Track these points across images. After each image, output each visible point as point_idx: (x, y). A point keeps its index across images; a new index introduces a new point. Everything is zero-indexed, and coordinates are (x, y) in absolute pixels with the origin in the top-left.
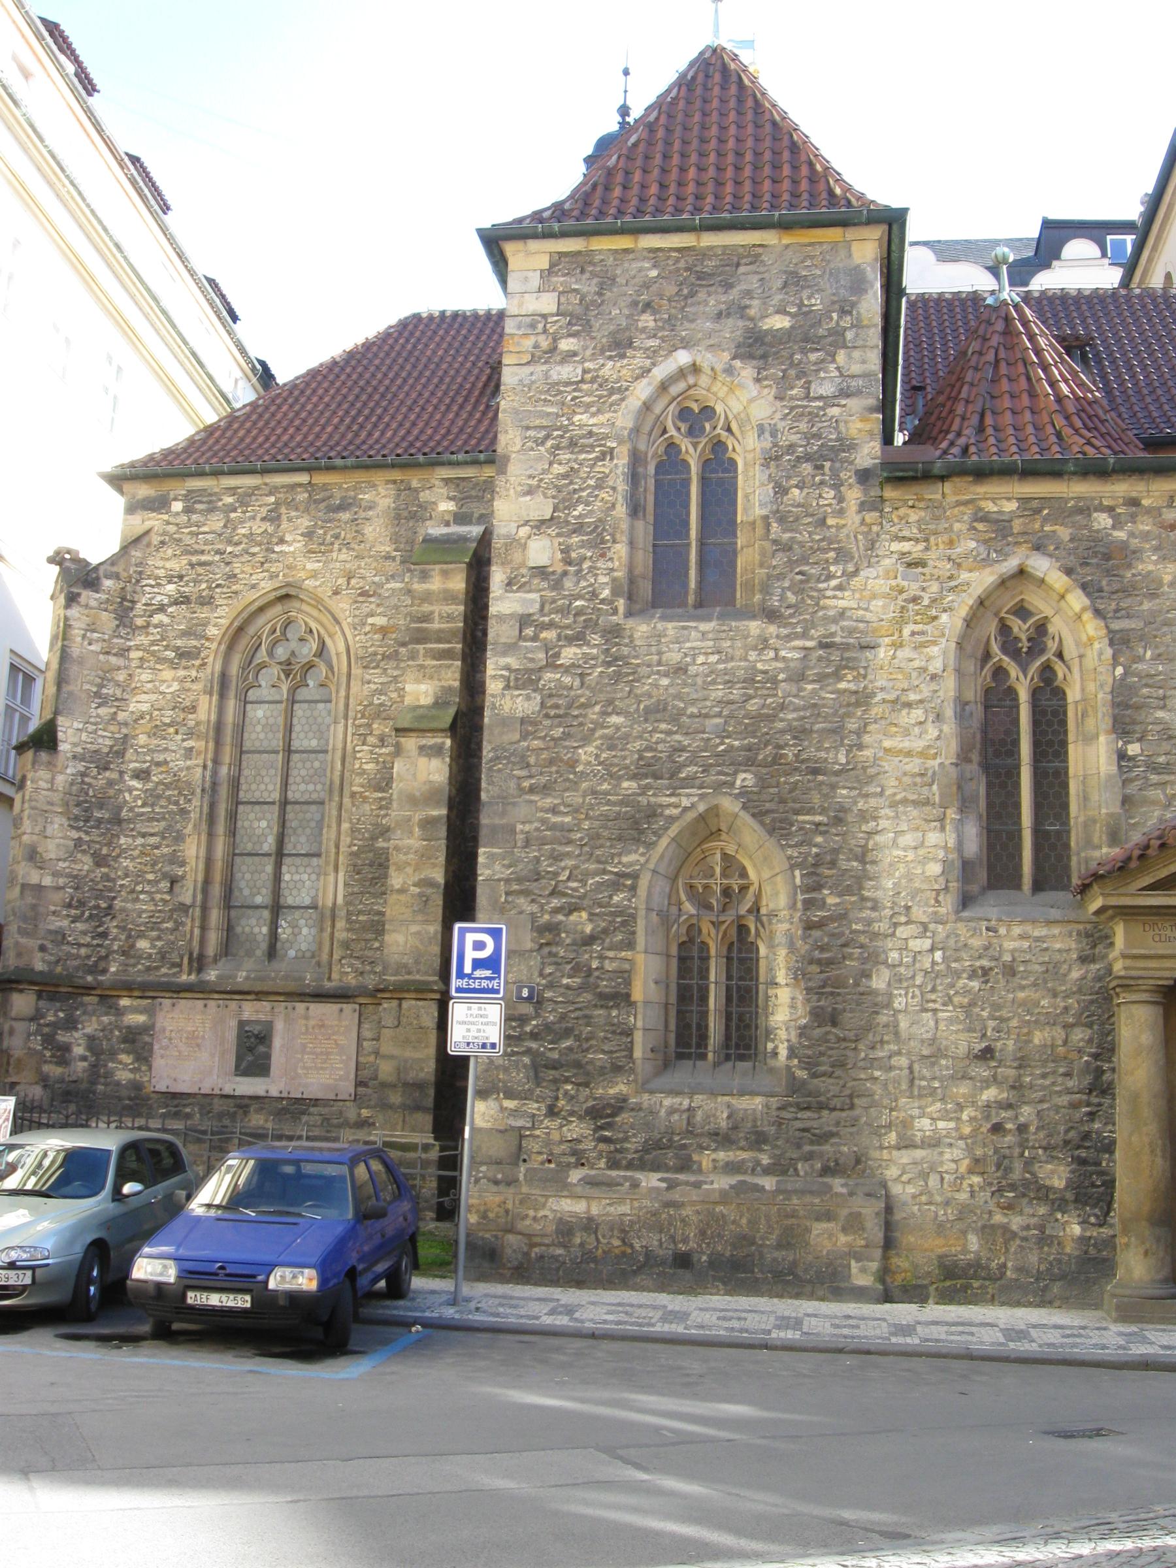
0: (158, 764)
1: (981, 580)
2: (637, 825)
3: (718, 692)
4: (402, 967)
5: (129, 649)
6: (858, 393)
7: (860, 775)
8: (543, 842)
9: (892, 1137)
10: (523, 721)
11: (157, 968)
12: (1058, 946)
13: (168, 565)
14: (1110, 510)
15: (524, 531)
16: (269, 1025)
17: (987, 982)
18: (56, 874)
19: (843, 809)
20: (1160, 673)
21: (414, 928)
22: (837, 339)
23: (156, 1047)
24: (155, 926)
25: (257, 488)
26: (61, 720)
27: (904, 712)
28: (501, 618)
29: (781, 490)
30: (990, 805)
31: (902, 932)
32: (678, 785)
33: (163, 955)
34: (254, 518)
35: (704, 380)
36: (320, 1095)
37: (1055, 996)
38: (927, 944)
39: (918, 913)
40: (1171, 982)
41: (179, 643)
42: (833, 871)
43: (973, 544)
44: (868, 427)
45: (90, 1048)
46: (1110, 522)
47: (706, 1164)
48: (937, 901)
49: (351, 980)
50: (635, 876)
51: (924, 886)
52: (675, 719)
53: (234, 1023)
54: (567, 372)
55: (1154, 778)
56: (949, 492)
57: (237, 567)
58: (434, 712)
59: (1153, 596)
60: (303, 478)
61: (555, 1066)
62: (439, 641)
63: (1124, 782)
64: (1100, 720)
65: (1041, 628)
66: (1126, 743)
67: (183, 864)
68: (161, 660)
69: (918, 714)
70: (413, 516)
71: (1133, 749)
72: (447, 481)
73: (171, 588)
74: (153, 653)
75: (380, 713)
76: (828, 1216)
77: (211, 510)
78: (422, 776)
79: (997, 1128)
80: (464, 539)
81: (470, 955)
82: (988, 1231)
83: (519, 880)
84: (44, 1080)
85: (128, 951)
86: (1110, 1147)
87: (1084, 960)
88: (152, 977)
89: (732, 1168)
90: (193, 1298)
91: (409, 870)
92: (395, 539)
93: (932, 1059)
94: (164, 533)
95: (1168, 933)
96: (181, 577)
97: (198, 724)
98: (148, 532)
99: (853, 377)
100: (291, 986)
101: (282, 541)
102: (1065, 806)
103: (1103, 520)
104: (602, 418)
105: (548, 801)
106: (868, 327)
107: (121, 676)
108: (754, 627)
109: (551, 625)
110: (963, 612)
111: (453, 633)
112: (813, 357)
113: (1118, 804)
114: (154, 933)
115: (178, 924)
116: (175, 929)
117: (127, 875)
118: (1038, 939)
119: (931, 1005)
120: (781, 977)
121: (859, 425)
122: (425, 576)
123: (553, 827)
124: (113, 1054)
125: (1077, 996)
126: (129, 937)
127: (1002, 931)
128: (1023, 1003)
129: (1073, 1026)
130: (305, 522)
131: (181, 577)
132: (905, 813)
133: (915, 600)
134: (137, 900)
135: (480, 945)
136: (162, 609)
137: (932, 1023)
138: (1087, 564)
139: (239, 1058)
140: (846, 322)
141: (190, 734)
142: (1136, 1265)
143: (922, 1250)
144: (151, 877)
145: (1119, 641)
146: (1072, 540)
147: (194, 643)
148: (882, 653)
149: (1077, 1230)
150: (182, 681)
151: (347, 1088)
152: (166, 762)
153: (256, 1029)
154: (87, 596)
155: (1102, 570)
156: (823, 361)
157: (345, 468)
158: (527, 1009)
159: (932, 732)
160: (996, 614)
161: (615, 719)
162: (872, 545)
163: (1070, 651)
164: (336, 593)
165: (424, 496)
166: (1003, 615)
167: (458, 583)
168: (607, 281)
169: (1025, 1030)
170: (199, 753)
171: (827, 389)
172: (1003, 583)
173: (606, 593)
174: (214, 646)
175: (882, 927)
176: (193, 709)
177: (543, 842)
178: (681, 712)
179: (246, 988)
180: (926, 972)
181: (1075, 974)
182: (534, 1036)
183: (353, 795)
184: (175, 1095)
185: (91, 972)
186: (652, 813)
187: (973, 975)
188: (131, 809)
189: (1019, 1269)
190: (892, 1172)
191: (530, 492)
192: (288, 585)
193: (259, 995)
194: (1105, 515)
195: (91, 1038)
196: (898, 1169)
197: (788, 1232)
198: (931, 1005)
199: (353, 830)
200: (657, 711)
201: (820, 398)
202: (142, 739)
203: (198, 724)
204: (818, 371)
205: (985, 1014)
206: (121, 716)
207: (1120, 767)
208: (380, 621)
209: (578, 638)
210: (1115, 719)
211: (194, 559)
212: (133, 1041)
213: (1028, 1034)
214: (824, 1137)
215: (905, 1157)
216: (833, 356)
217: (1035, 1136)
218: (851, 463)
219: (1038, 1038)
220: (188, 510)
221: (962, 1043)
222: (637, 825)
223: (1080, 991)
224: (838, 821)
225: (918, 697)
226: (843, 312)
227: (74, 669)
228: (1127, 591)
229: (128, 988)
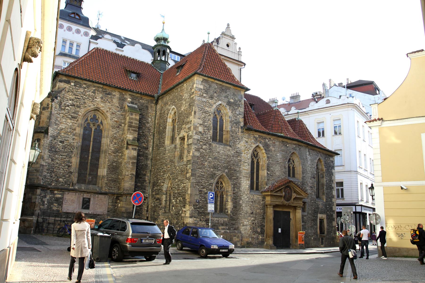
0: (66, 140)
1: (254, 146)
2: (213, 176)
3: (224, 157)
4: (127, 190)
5: (60, 113)
7: (240, 172)
8: (200, 177)
9: (242, 225)
10: (197, 157)
11: (64, 185)
13: (70, 96)
15: (198, 125)
16: (89, 199)
18: (46, 163)
19: (238, 177)
21: (130, 183)
22: (239, 106)
23: (64, 202)
24: (64, 176)
25: (91, 85)
26: (49, 128)
28: (194, 139)
29: (232, 127)
31: (244, 195)
32: (218, 171)
33: (66, 182)
34: (90, 91)
35: (221, 106)
36: (100, 214)
38: (246, 197)
39: (246, 193)
41: (72, 114)
42: (236, 186)
45: (47, 202)
47: (220, 228)
49: (107, 191)
50: (212, 184)
52: (218, 160)
53: (82, 198)
54: (204, 100)
56: (251, 133)
57: (86, 101)
58: (134, 142)
60: (101, 86)
61: (201, 213)
62: (134, 128)
64: (265, 167)
65: (257, 154)
67: (71, 163)
68: (68, 117)
69: (246, 164)
70: (123, 100)
71: (269, 173)
72: (130, 95)
73: (71, 102)
74: (66, 116)
75: (115, 138)
76: (235, 236)
77: (81, 87)
78: (132, 154)
79: (253, 223)
80: (135, 108)
81: (210, 197)
82: (252, 238)
83: (197, 183)
84: (40, 209)
85: (57, 181)
86: (264, 226)
87: (263, 201)
88: (63, 187)
89: (223, 229)
90: (221, 250)
91: (129, 171)
92: (119, 104)
93: (246, 214)
94: (69, 89)
96: (73, 100)
97: (76, 133)
98: (66, 88)
100: (95, 191)
101: (96, 98)
102: (258, 179)
103: (267, 140)
104: (209, 109)
105: (201, 170)
107: (59, 120)
108: (228, 147)
109: (202, 142)
111: (137, 127)
114: (64, 177)
115: (69, 176)
116: (69, 177)
117: (57, 164)
120: (229, 200)
122: (132, 115)
123: (202, 175)
124: (52, 203)
126: (57, 177)
130: (101, 95)
131: (73, 100)
133: (247, 147)
134: (60, 169)
135: (211, 195)
136: (68, 106)
139: (83, 206)
140: (240, 103)
141: (74, 135)
142: (271, 242)
143: (245, 240)
144: (63, 165)
147: (76, 115)
148: (243, 154)
149: (261, 237)
150: (73, 123)
151: (106, 212)
152: (68, 140)
153: (87, 199)
154: (55, 100)
155: (266, 147)
157: (113, 87)
158: (197, 204)
161: (210, 159)
162: (242, 138)
163: (261, 157)
164: (107, 112)
165: (125, 96)
167: (138, 117)
168: (210, 86)
170: (76, 139)
171: (238, 113)
173: (209, 138)
174: (80, 117)
175: (242, 194)
176: (75, 130)
177: (200, 177)
178: (219, 159)
179: (85, 190)
182: (198, 208)
183: (109, 154)
184: (67, 213)
185: (49, 185)
186: (215, 174)
188: (59, 149)
189: (255, 243)
190: (242, 230)
191: (199, 119)
192: (97, 108)
193: (88, 193)
195: (48, 200)
196: (242, 229)
197: (231, 238)
199: (109, 161)
200: (215, 158)
202: (63, 134)
203: (76, 133)
206: (58, 128)
208: (116, 120)
209: (205, 145)
211: (76, 97)
212: (57, 201)
214: (234, 224)
215: (243, 227)
217: (257, 225)
219: (258, 211)
220: (75, 85)
221: (250, 211)
222: (213, 176)
224: (237, 178)
226: (240, 102)
227: (52, 116)
228: (269, 151)
229: (58, 189)
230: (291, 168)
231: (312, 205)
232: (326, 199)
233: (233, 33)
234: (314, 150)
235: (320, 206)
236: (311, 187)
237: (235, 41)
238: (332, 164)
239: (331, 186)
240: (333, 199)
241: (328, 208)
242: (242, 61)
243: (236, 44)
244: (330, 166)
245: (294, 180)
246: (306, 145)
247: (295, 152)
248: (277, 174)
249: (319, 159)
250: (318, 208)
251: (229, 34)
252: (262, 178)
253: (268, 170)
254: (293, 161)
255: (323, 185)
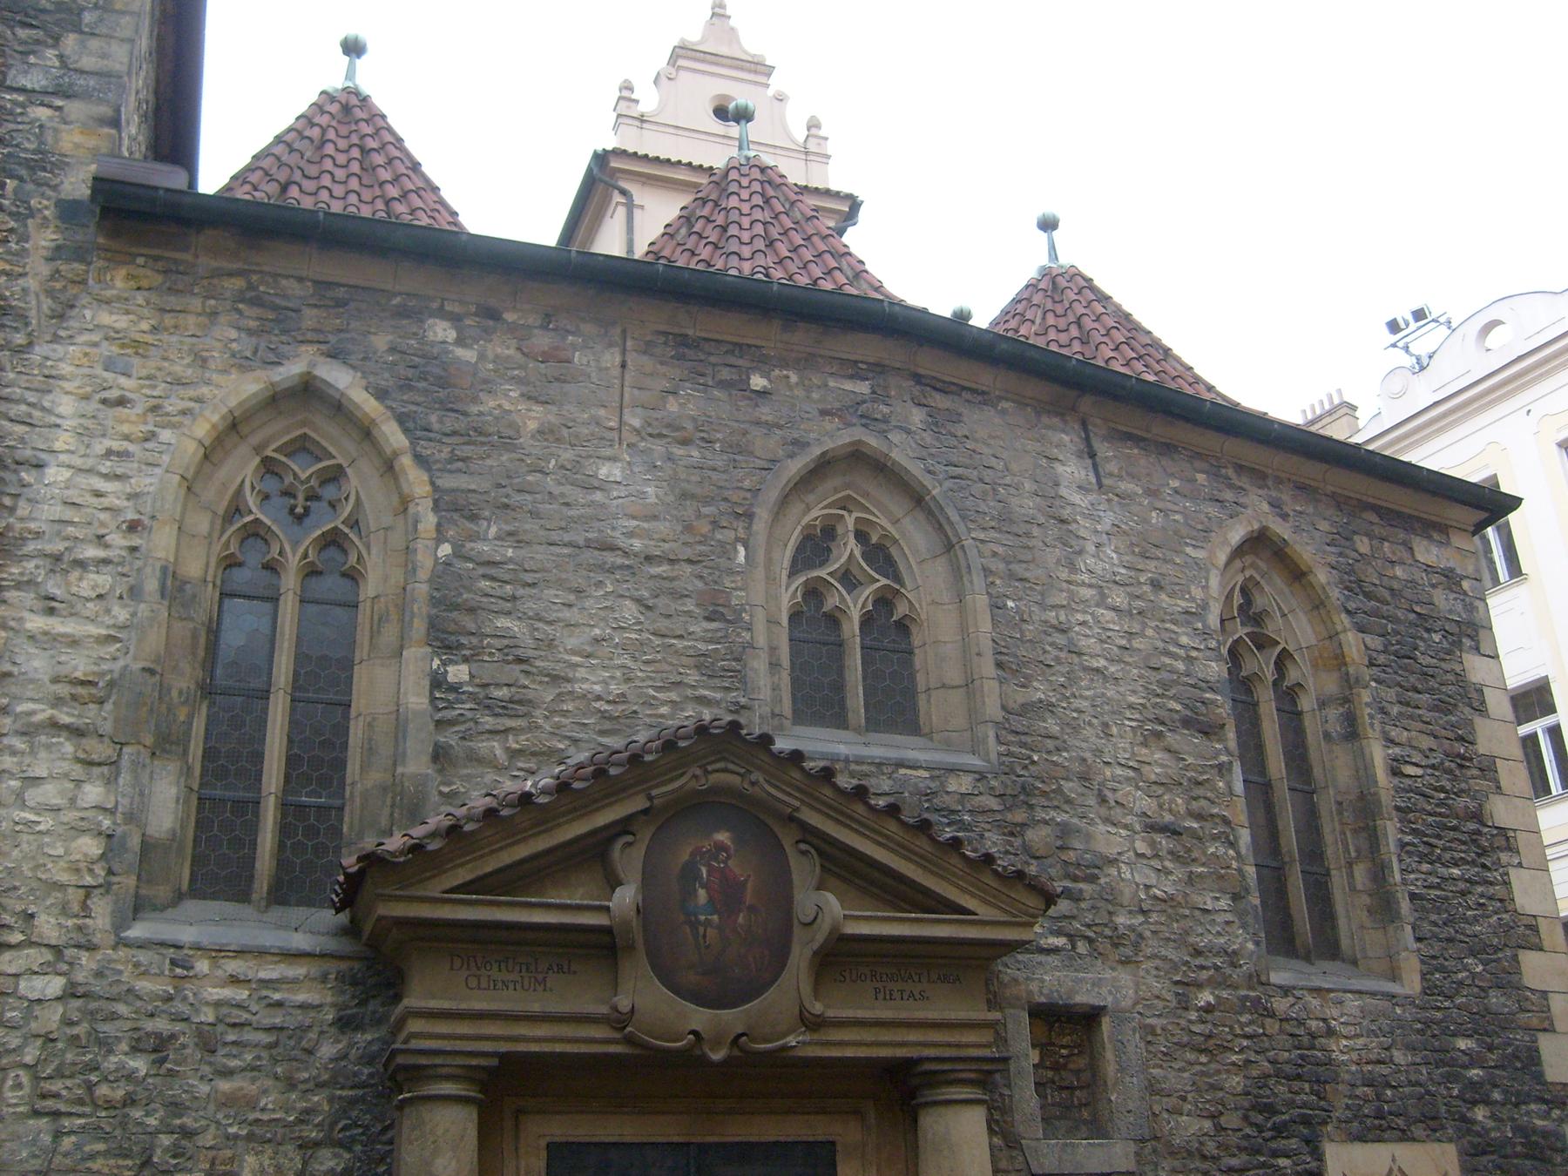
6: (85, 95)
12: (301, 997)
14: (455, 319)
17: (163, 1060)
20: (511, 560)
27: (76, 574)
30: (209, 754)
37: (291, 1085)
38: (55, 985)
39: (49, 926)
40: (494, 1062)
43: (234, 334)
44: (92, 142)
46: (452, 335)
48: (84, 906)
51: (64, 878)
55: (488, 721)
59: (512, 448)
63: (439, 724)
66: (444, 664)
71: (458, 673)
95: (495, 973)
99: (82, 72)
103: (442, 331)
106: (123, 13)
110: (202, 429)
112: (23, 33)
113: (426, 758)
118: (266, 983)
119: (50, 1104)
121: (78, 138)
125: (326, 1093)
127: (203, 966)
128: (228, 1101)
129: (317, 1144)
132: (48, 747)
137: (47, 1139)
138: (411, 388)
145: (451, 507)
146: (393, 350)
156: (38, 42)
159: (121, 614)
160: (258, 449)
166: (269, 452)
169: (229, 1153)
172: (275, 401)
180: (49, 1040)
181: (327, 1050)
187: (135, 1050)
194: (445, 324)
198: (50, 1104)
201: (22, 90)
204: (26, 54)
205: (152, 1121)
207: (433, 699)
210: (433, 625)
213: (232, 1160)
216: (56, 40)
218: (55, 188)
223: (332, 1083)
225: (101, 553)
230: (852, 627)
231: (1210, 1047)
232: (1430, 965)
233: (752, 43)
234: (1167, 448)
235: (1339, 1050)
236: (1173, 832)
237: (776, 83)
238: (1442, 600)
239: (1477, 816)
240: (1529, 959)
241: (1474, 1060)
242: (834, 187)
243: (780, 99)
244: (1425, 621)
245: (877, 752)
246: (1036, 389)
247: (873, 441)
248: (591, 681)
249: (1259, 543)
250: (1313, 1071)
251: (724, 51)
252: (370, 750)
253: (445, 642)
254: (880, 555)
255: (1365, 808)
